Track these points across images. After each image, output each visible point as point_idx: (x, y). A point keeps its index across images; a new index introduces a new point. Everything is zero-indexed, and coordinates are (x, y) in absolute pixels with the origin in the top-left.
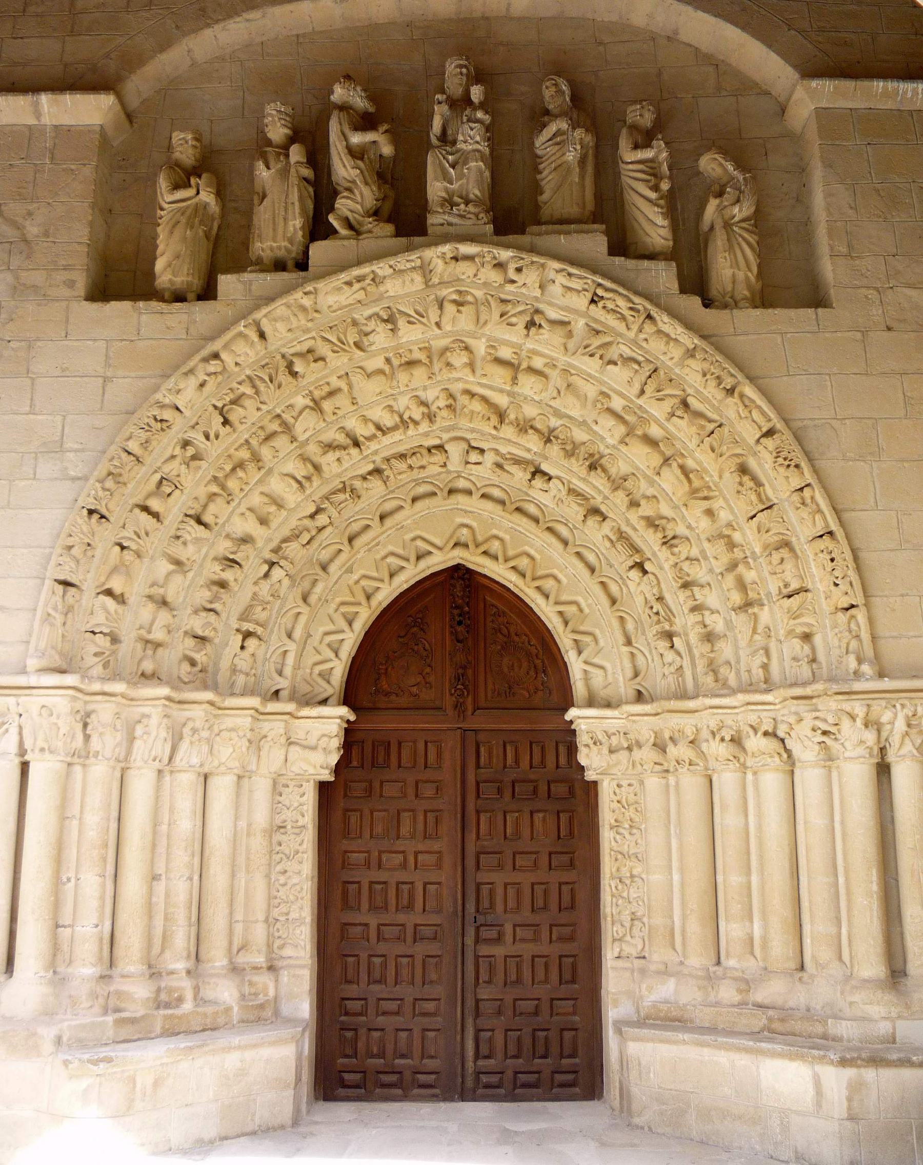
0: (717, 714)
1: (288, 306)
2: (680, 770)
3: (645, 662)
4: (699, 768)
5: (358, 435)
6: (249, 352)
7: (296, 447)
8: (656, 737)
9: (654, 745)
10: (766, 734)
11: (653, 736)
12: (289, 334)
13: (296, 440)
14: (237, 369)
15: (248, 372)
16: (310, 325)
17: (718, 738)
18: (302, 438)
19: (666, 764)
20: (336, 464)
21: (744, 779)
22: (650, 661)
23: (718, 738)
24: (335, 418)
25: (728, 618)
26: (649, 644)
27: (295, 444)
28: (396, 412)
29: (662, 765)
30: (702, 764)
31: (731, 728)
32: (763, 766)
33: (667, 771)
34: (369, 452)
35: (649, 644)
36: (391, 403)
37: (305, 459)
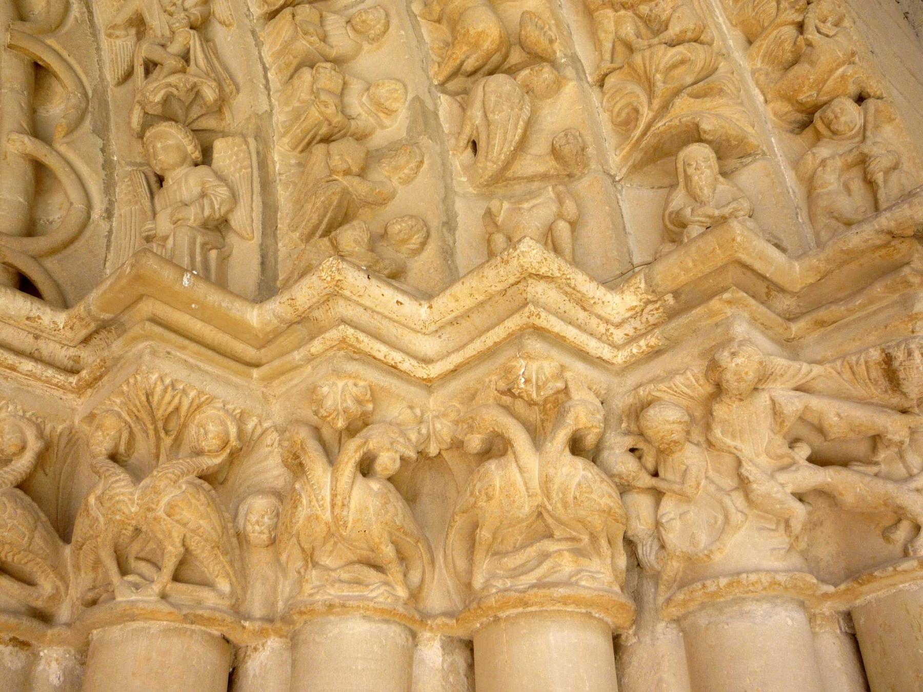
0: (369, 359)
2: (125, 596)
3: (79, 205)
4: (209, 597)
8: (41, 458)
9: (23, 486)
10: (576, 446)
11: (34, 445)
17: (351, 454)
19: (47, 585)
21: (409, 656)
22: (96, 214)
23: (351, 454)
25: (429, 104)
26: (108, 165)
29: (29, 582)
30: (224, 586)
31: (400, 428)
32: (540, 585)
33: (43, 617)
35: (108, 165)
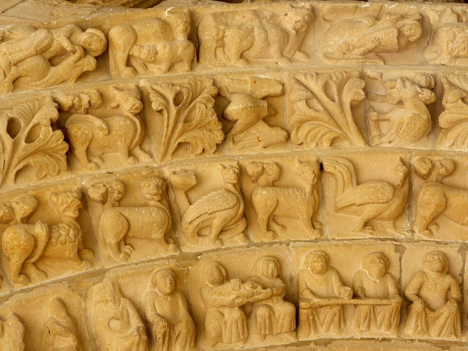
1: (256, 14)
5: (303, 287)
6: (159, 47)
7: (173, 257)
12: (240, 65)
13: (178, 245)
14: (127, 71)
15: (143, 83)
16: (283, 63)
18: (190, 247)
20: (236, 314)
24: (267, 238)
27: (170, 250)
28: (393, 277)
34: (313, 337)
36: (389, 250)
37: (178, 284)
